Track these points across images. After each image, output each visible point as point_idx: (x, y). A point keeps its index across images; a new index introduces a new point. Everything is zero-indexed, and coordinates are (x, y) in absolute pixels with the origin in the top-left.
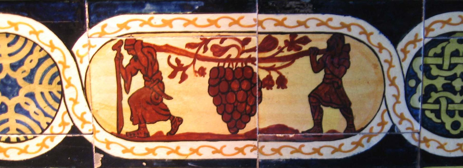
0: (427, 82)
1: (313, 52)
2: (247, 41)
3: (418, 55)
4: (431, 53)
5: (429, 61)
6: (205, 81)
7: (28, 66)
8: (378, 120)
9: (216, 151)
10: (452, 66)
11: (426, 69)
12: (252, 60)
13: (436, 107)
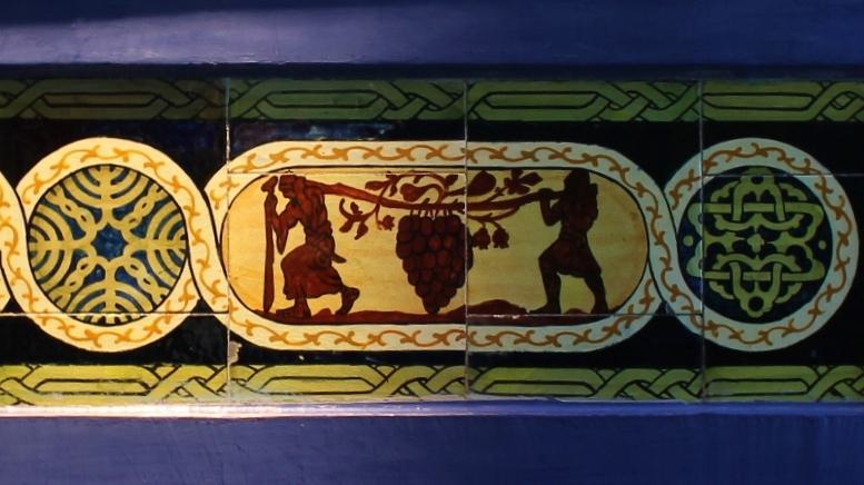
0: (710, 239)
1: (545, 195)
3: (695, 200)
5: (713, 208)
7: (139, 213)
8: (640, 294)
11: (708, 220)
12: (459, 206)
13: (725, 276)
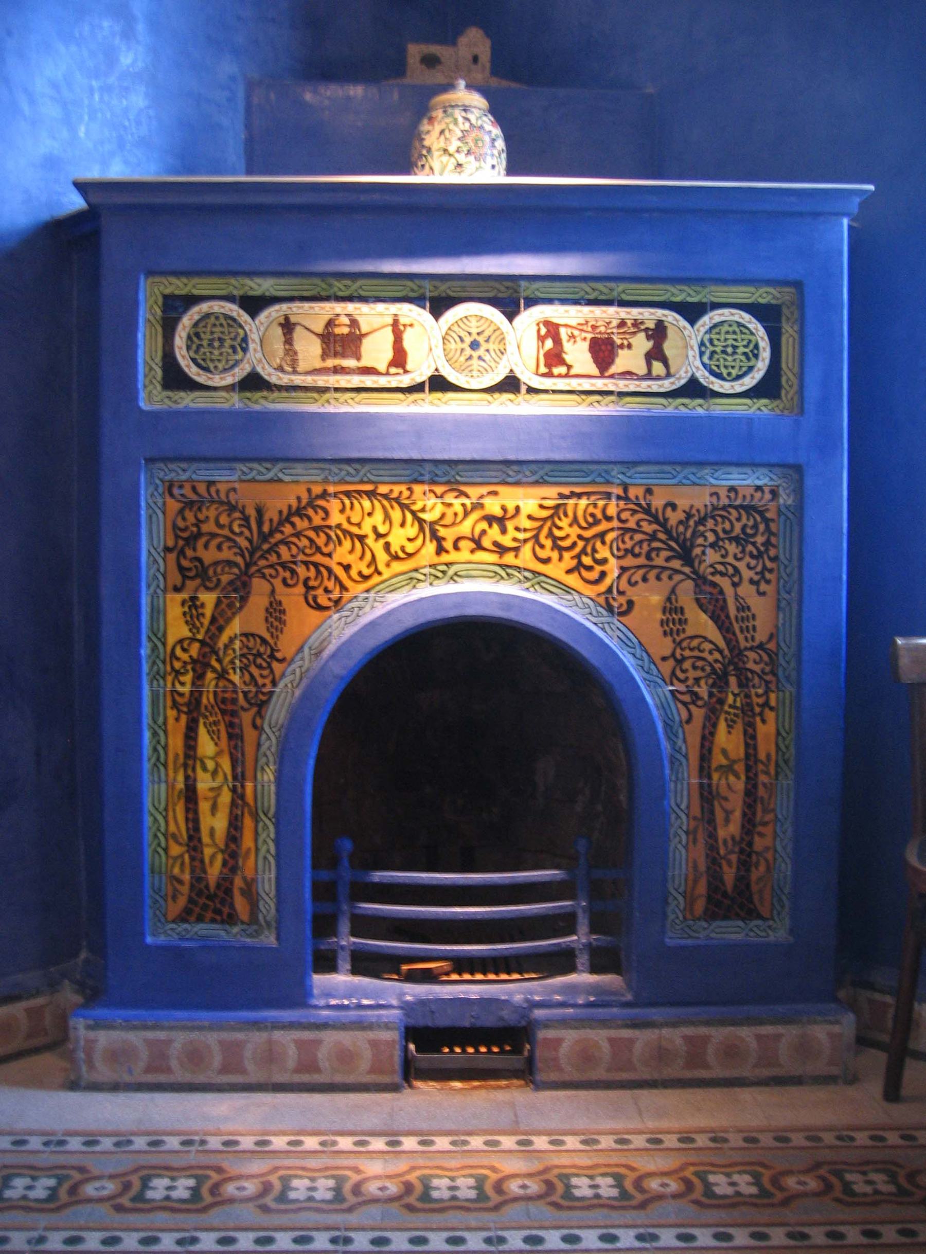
0: (712, 348)
1: (647, 330)
2: (609, 323)
3: (706, 333)
4: (714, 331)
5: (713, 336)
6: (586, 345)
7: (486, 334)
8: (684, 369)
9: (593, 385)
10: (726, 340)
11: (711, 341)
12: (613, 333)
13: (717, 363)
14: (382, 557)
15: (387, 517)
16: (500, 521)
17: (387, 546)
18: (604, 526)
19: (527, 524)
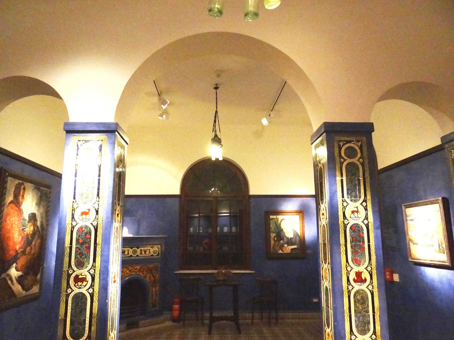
14: (126, 274)
15: (126, 270)
16: (136, 269)
17: (126, 273)
18: (145, 269)
19: (138, 269)
